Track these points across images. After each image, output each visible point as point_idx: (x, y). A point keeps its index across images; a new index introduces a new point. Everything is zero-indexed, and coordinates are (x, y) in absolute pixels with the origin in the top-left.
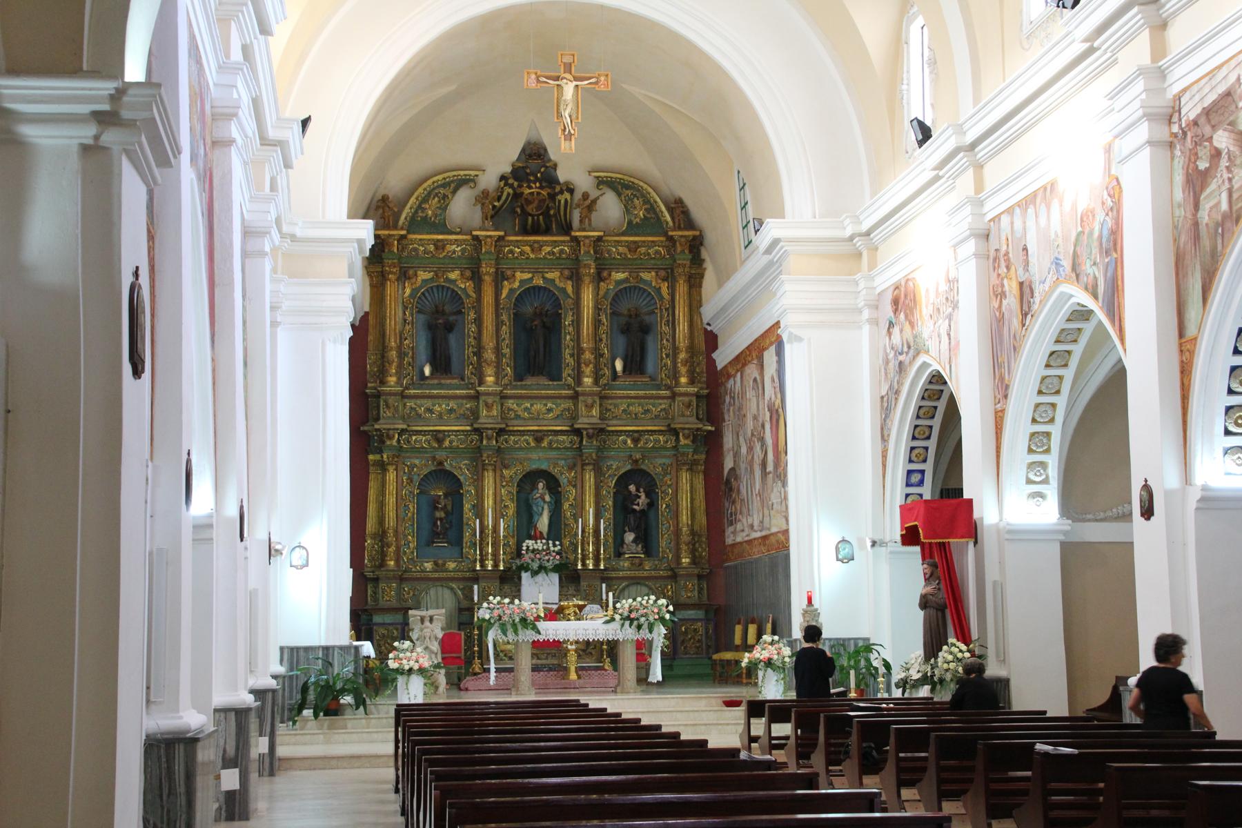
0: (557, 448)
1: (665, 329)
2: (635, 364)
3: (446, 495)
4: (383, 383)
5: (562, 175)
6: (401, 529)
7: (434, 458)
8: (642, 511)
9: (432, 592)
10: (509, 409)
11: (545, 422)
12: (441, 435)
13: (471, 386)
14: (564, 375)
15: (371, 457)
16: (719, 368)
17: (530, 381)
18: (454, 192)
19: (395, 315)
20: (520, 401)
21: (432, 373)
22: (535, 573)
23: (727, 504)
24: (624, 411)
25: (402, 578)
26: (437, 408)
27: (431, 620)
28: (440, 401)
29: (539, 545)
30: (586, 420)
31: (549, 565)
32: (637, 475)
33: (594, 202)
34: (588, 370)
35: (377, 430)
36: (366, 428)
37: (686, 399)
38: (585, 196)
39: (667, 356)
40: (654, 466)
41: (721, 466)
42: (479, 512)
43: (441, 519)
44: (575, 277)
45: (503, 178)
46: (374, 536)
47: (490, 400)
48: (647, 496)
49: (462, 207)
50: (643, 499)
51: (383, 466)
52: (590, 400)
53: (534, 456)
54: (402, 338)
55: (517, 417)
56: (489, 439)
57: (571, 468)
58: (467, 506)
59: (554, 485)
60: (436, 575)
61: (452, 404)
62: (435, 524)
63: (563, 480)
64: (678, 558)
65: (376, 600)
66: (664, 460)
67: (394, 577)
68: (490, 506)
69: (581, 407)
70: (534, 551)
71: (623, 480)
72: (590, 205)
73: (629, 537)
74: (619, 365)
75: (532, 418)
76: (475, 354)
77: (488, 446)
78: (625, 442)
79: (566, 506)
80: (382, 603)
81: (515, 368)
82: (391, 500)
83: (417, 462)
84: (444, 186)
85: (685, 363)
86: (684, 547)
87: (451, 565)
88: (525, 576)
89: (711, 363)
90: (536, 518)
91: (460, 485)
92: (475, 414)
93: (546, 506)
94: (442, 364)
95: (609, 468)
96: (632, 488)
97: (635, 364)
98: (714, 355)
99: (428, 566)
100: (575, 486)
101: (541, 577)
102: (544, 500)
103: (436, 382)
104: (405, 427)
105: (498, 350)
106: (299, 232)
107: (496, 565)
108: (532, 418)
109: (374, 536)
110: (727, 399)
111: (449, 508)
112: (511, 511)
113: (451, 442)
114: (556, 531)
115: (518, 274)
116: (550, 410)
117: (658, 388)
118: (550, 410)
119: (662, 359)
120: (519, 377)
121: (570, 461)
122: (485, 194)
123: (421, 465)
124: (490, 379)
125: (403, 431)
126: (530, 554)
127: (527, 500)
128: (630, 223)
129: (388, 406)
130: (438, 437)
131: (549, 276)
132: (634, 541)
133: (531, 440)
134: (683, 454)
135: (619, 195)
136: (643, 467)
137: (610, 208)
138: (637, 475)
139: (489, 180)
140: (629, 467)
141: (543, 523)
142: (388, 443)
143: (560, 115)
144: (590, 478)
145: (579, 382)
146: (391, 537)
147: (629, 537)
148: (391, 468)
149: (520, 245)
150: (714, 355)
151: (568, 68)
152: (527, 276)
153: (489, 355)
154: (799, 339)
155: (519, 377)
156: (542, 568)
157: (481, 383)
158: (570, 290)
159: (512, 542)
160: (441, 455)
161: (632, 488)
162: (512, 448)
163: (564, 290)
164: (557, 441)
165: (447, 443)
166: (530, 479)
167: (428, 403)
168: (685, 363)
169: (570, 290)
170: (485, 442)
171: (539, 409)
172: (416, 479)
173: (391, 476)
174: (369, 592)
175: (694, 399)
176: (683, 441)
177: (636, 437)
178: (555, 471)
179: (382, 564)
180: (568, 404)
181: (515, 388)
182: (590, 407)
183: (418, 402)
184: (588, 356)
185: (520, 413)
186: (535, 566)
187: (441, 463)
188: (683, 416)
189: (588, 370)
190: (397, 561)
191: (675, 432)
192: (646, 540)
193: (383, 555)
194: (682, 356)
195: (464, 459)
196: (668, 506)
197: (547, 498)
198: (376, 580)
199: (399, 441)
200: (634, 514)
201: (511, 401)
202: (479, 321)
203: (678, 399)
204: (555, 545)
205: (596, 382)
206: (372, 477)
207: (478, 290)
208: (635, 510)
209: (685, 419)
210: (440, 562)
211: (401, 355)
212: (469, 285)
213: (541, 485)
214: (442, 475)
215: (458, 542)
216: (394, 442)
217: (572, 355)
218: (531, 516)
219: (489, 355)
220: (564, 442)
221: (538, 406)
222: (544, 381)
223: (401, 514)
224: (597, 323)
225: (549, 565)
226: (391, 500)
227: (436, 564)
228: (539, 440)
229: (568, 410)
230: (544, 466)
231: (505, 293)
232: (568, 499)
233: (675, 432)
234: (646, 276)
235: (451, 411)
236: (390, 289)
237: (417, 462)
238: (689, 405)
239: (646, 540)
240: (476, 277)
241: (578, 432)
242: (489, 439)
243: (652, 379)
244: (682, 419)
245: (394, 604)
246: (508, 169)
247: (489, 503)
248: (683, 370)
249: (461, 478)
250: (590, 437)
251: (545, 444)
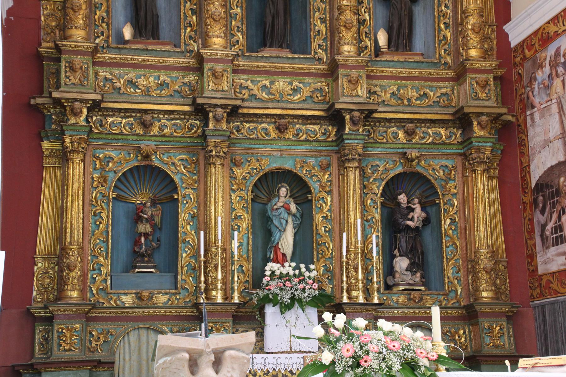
0: (306, 141)
2: (401, 38)
3: (154, 203)
6: (88, 248)
7: (138, 149)
8: (417, 228)
9: (133, 336)
10: (242, 87)
11: (292, 106)
12: (148, 117)
14: (314, 46)
15: (46, 145)
16: (513, 44)
17: (267, 52)
20: (255, 77)
21: (134, 36)
22: (285, 308)
23: (539, 218)
24: (393, 94)
25: (90, 315)
26: (142, 82)
27: (217, 364)
28: (147, 72)
29: (288, 269)
30: (348, 100)
31: (305, 297)
32: (411, 180)
34: (348, 36)
35: (57, 102)
36: (39, 100)
37: (483, 77)
39: (447, 26)
40: (435, 168)
41: (526, 170)
42: (202, 222)
43: (146, 235)
46: (48, 257)
47: (219, 67)
48: (423, 209)
50: (418, 213)
51: (64, 157)
52: (354, 73)
53: (275, 149)
55: (254, 97)
57: (324, 168)
58: (184, 217)
60: (140, 312)
61: (164, 77)
62: (137, 242)
63: (314, 185)
64: (477, 290)
65: (49, 351)
66: (444, 162)
67: (78, 315)
68: (219, 213)
69: (343, 82)
70: (281, 277)
71: (392, 187)
73: (402, 263)
74: (382, 38)
75: (271, 101)
76: (194, 12)
78: (396, 136)
79: (319, 218)
80: (57, 355)
81: (248, 38)
83: (113, 154)
85: (477, 30)
86: (483, 276)
87: (161, 299)
88: (271, 311)
89: (503, 37)
90: (276, 235)
91: (175, 189)
92: (196, 90)
93: (290, 220)
95: (375, 168)
97: (401, 38)
98: (507, 28)
99: (128, 300)
100: (329, 192)
101: (295, 313)
102: (288, 210)
103: (140, 47)
104: (98, 97)
107: (227, 297)
108: (271, 101)
109: (48, 257)
110: (541, 75)
111: (158, 220)
113: (161, 129)
114: (304, 252)
116: (296, 91)
117: (435, 65)
118: (296, 91)
119: (440, 30)
121: (324, 160)
123: (121, 160)
124: (217, 41)
126: (277, 281)
127: (265, 211)
129: (72, 68)
130: (144, 119)
132: (411, 268)
133: (271, 128)
134: (478, 150)
136: (419, 169)
138: (411, 180)
140: (400, 169)
141: (287, 242)
142: (72, 121)
144: (353, 179)
146: (74, 259)
147: (402, 263)
148: (76, 157)
150: (507, 28)
156: (295, 300)
157: (205, 45)
159: (247, 266)
160: (148, 145)
161: (402, 198)
162: (245, 138)
164: (306, 132)
165: (155, 130)
166: (268, 182)
167: (131, 74)
168: (477, 30)
170: (211, 126)
171: (282, 85)
172: (112, 178)
173: (76, 169)
174: (38, 338)
175: (491, 77)
176: (477, 132)
177: (410, 127)
178: (303, 173)
179: (60, 295)
180: (321, 83)
181: (249, 57)
182: (354, 83)
183: (116, 71)
184: (349, 16)
185: (255, 92)
186: (286, 297)
187: (147, 157)
188: (478, 99)
189: (348, 36)
191: (462, 120)
193: (61, 284)
194: (472, 21)
195: (179, 151)
196: (453, 221)
197: (293, 208)
198: (49, 320)
200: (409, 232)
201: (244, 77)
203: (469, 76)
204: (308, 270)
205: (360, 50)
206: (47, 172)
208: (408, 226)
209: (481, 103)
210: (145, 293)
213: (283, 191)
214: (147, 172)
215: (171, 266)
216: (82, 120)
217: (323, 21)
218: (268, 234)
220: (315, 132)
221: (281, 85)
222: (285, 53)
223: (90, 227)
225: (305, 297)
226: (75, 204)
227: (139, 297)
228: (281, 129)
229: (321, 90)
230: (288, 165)
232: (321, 208)
233: (462, 120)
235: (162, 85)
237: (113, 154)
238: (484, 85)
241: (335, 117)
244: (476, 103)
245: (77, 355)
248: (474, 39)
249: (176, 178)
250: (354, 122)
251: (289, 135)
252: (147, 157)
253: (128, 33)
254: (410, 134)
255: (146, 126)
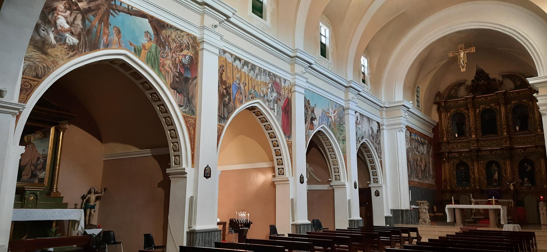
1: (532, 116)
2: (524, 127)
4: (443, 139)
5: (491, 77)
13: (468, 139)
18: (459, 87)
19: (445, 123)
33: (502, 82)
38: (499, 81)
44: (499, 104)
45: (472, 81)
49: (462, 92)
50: (529, 168)
51: (445, 163)
54: (448, 127)
56: (474, 153)
58: (471, 172)
59: (498, 165)
72: (501, 83)
73: (526, 179)
74: (517, 128)
77: (477, 154)
78: (521, 151)
82: (447, 171)
84: (455, 85)
94: (461, 133)
96: (526, 164)
100: (505, 165)
105: (476, 128)
106: (387, 106)
112: (484, 173)
115: (481, 106)
120: (484, 134)
122: (468, 86)
123: (456, 161)
125: (449, 153)
128: (515, 86)
131: (492, 105)
135: (510, 79)
137: (509, 85)
139: (469, 83)
143: (460, 62)
144: (508, 162)
145: (502, 134)
147: (526, 179)
149: (480, 97)
151: (461, 49)
152: (483, 106)
153: (473, 129)
154: (545, 114)
155: (484, 134)
158: (498, 108)
161: (526, 164)
163: (496, 109)
169: (498, 108)
172: (455, 165)
173: (447, 164)
190: (450, 187)
192: (532, 181)
199: (448, 155)
202: (469, 121)
207: (469, 112)
211: (448, 132)
212: (466, 112)
214: (461, 164)
219: (473, 129)
224: (507, 117)
231: (477, 111)
234: (524, 101)
236: (443, 115)
239: (532, 181)
240: (468, 109)
242: (474, 153)
243: (529, 131)
246: (474, 78)
247: (476, 170)
252: (461, 160)
253: (457, 135)
254: (525, 150)
255: (461, 154)
